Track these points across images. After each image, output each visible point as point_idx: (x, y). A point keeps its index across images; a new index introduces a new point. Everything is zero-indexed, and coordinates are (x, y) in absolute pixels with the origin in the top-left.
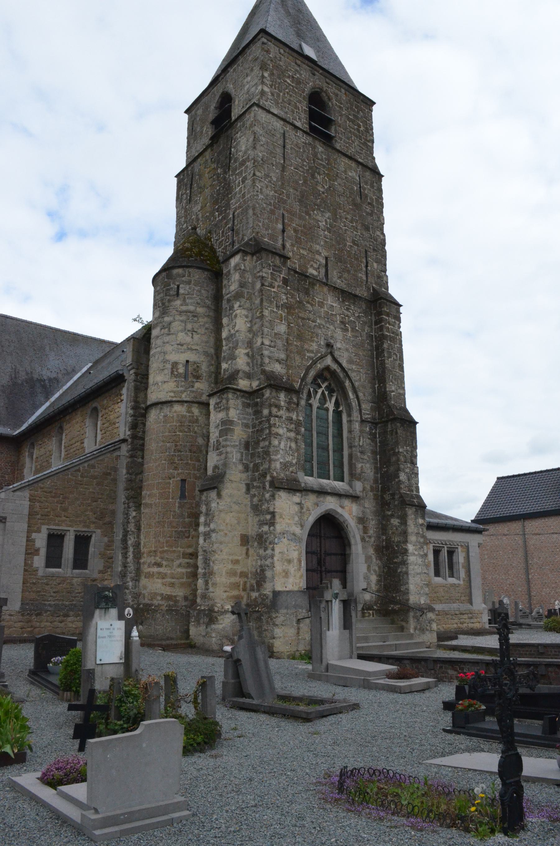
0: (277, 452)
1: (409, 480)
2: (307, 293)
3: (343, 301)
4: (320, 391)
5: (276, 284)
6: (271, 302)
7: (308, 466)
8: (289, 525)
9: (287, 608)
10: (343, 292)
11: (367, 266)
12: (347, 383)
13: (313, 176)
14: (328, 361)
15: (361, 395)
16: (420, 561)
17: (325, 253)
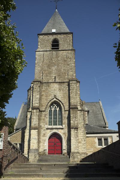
0: (33, 122)
1: (74, 122)
2: (49, 86)
3: (60, 85)
4: (54, 107)
5: (37, 88)
6: (35, 92)
7: (51, 123)
8: (34, 136)
9: (32, 153)
10: (60, 82)
11: (68, 74)
12: (60, 103)
13: (52, 60)
14: (55, 99)
15: (65, 105)
16: (75, 141)
17: (54, 76)
